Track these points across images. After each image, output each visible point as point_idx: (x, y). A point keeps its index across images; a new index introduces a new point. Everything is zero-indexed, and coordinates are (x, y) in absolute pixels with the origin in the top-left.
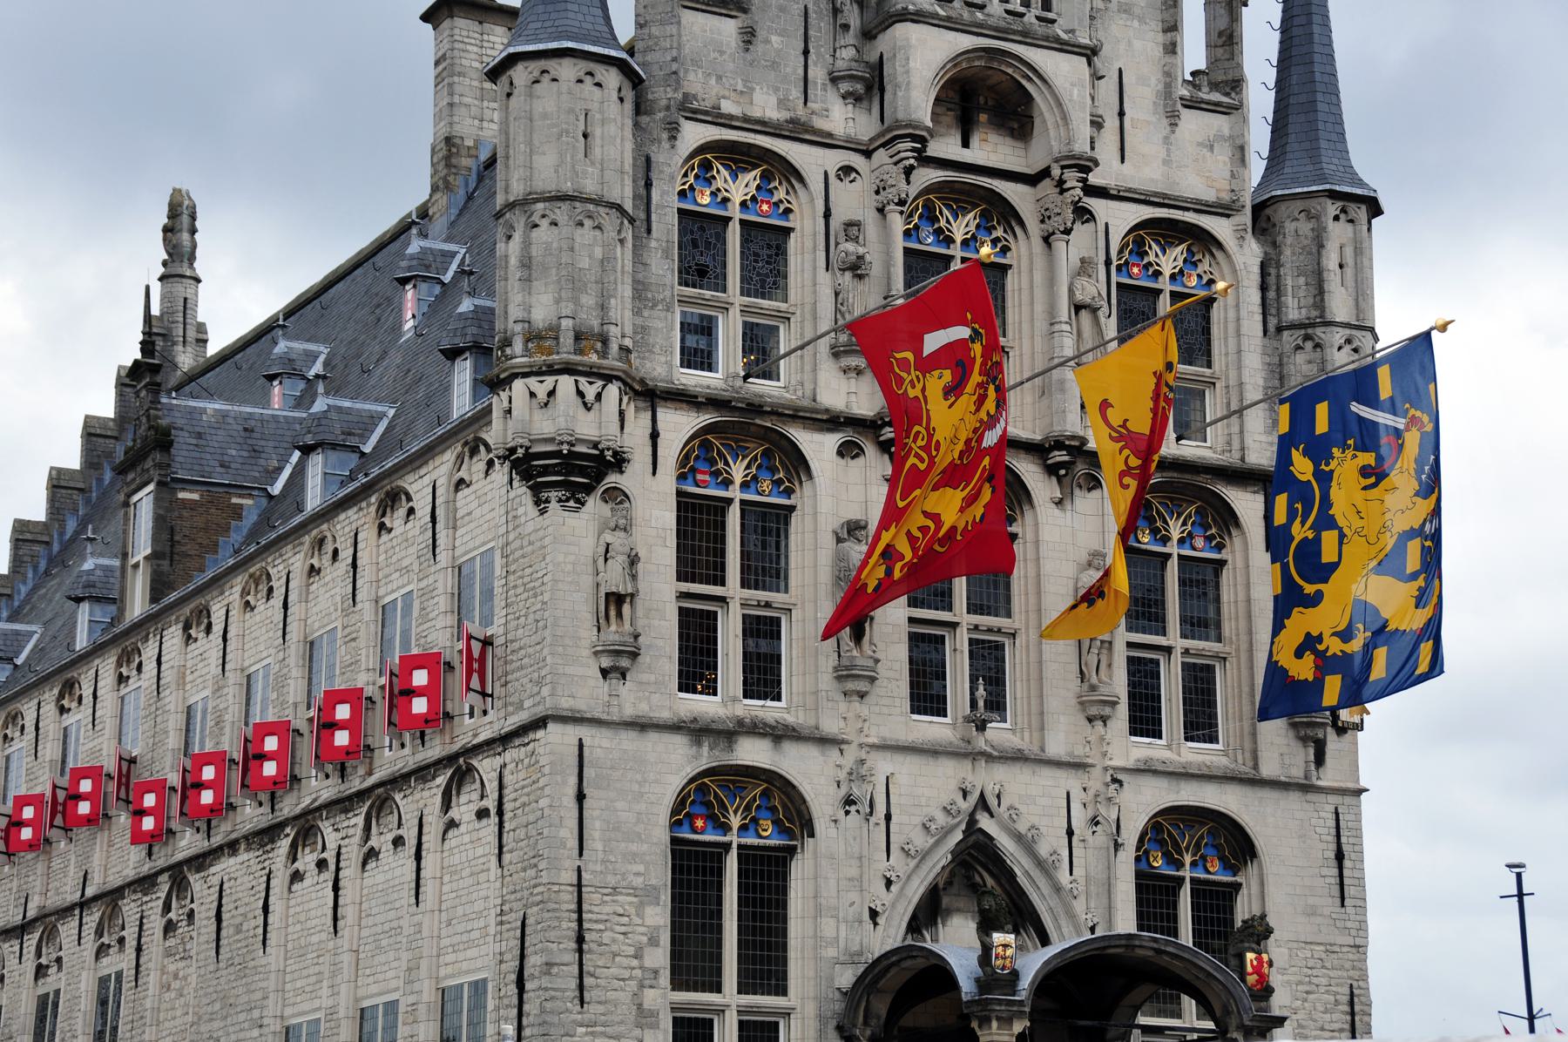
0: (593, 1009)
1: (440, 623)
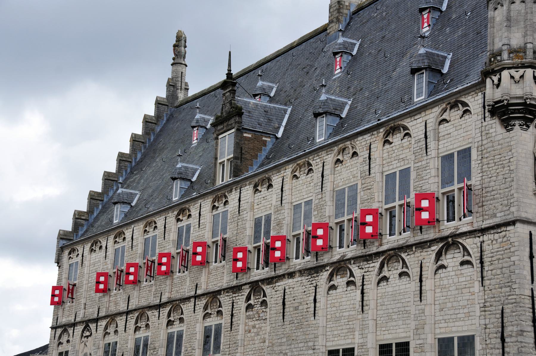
1: (432, 181)
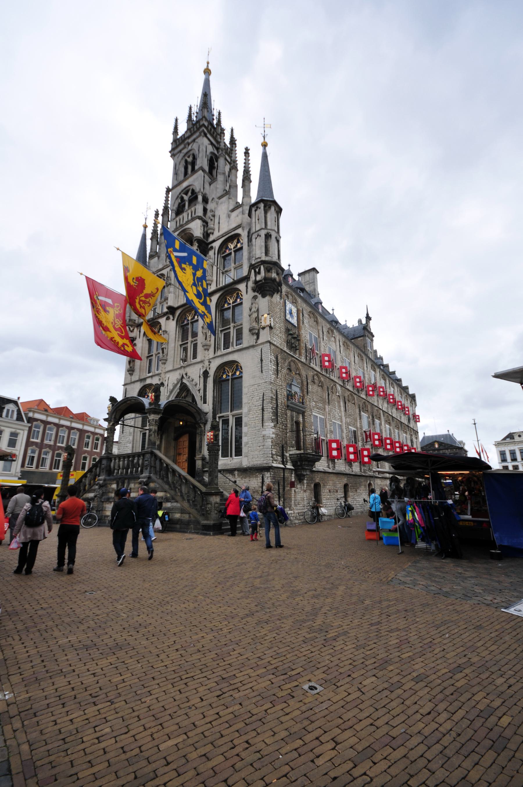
0: (125, 434)
